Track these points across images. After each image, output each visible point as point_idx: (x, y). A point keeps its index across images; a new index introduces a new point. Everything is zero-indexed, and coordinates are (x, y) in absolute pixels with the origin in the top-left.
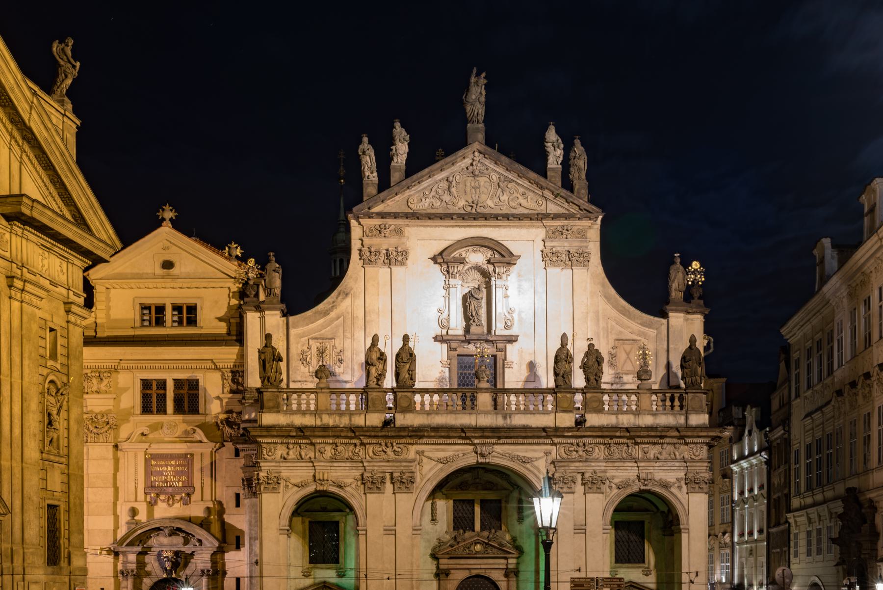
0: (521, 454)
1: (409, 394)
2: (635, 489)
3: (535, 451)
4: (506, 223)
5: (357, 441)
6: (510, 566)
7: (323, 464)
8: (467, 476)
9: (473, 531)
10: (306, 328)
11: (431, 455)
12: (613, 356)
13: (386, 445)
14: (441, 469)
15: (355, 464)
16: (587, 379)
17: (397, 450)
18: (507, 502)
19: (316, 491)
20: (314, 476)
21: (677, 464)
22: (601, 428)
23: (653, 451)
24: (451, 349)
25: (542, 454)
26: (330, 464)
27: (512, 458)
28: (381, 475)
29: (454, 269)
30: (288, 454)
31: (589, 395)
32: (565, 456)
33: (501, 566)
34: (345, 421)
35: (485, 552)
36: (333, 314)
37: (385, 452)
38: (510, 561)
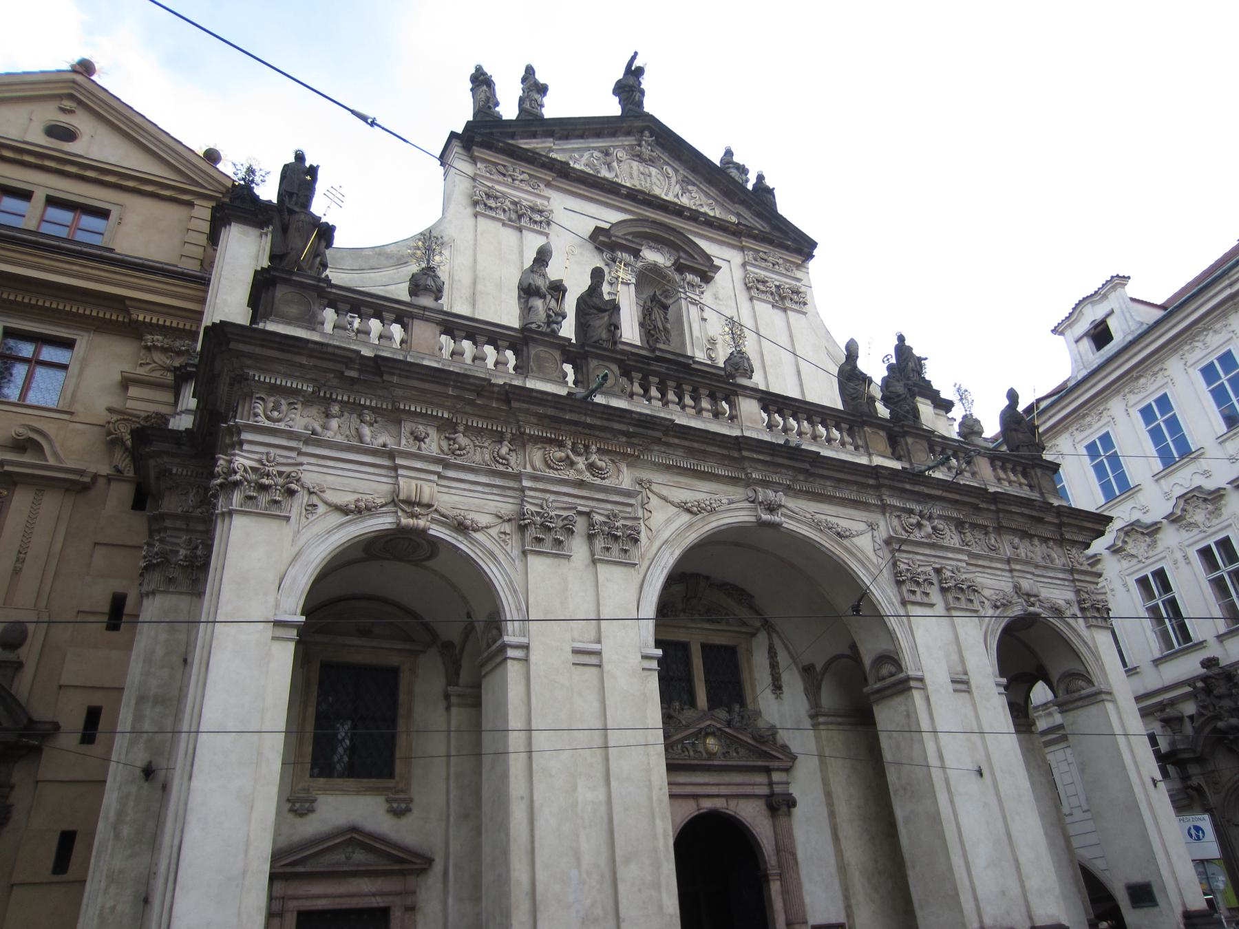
0: (829, 518)
5: (509, 431)
6: (777, 789)
7: (419, 465)
9: (693, 703)
11: (664, 491)
14: (691, 525)
15: (498, 482)
17: (600, 463)
18: (750, 652)
20: (396, 492)
21: (1061, 576)
23: (1024, 549)
25: (863, 527)
26: (439, 469)
27: (817, 526)
28: (565, 514)
30: (325, 427)
35: (726, 754)
37: (572, 464)
38: (776, 777)
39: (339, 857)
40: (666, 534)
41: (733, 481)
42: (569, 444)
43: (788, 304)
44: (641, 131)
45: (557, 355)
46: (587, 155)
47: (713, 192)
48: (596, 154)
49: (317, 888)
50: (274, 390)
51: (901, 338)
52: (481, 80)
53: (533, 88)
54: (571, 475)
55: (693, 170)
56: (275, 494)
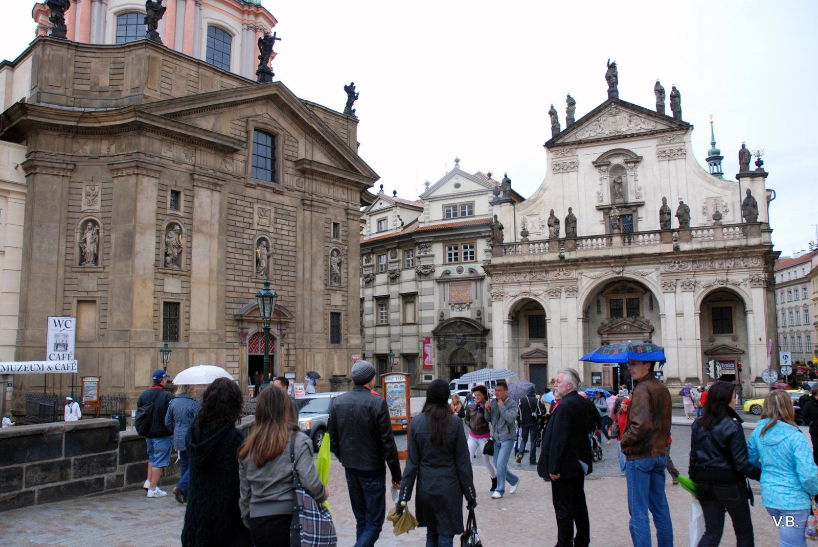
0: (640, 271)
1: (573, 241)
2: (715, 287)
3: (649, 268)
4: (633, 139)
8: (616, 286)
9: (622, 317)
10: (524, 211)
11: (587, 274)
12: (704, 208)
13: (559, 270)
14: (593, 283)
16: (681, 223)
18: (642, 300)
19: (523, 300)
22: (688, 252)
24: (605, 214)
25: (654, 270)
29: (604, 168)
31: (681, 233)
32: (668, 270)
33: (640, 338)
34: (537, 259)
35: (630, 330)
36: (538, 202)
38: (645, 334)
39: (536, 354)
40: (587, 286)
41: (607, 267)
42: (558, 270)
43: (676, 157)
44: (611, 103)
45: (557, 243)
46: (590, 126)
47: (643, 116)
48: (595, 123)
49: (532, 360)
50: (496, 274)
51: (743, 146)
52: (553, 113)
53: (571, 102)
54: (560, 277)
55: (634, 110)
56: (499, 296)
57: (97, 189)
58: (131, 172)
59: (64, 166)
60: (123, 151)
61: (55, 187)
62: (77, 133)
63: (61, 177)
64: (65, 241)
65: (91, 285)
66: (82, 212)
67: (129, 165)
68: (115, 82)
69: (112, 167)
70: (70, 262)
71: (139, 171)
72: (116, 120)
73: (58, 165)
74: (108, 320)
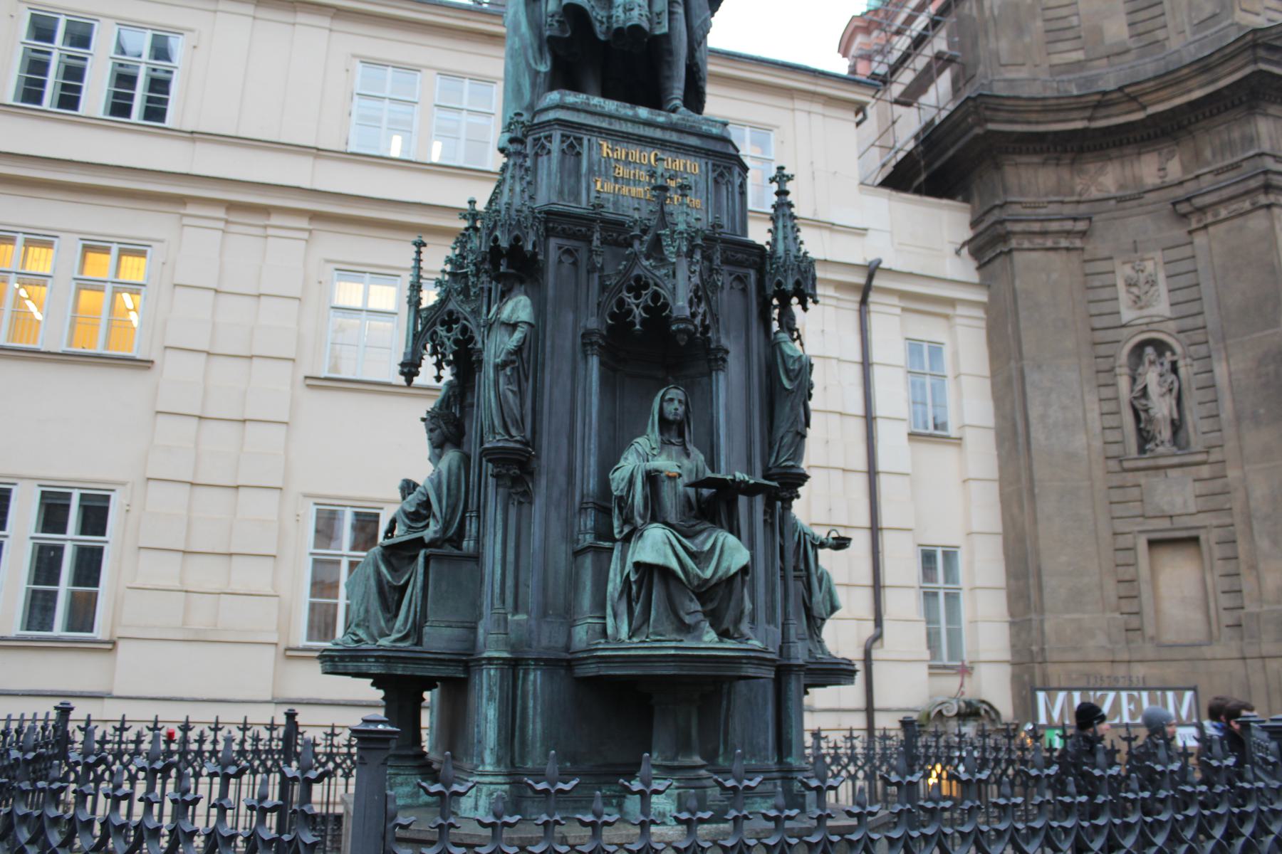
57: (1149, 266)
58: (1247, 205)
59: (1068, 225)
60: (1208, 164)
61: (1055, 276)
62: (1082, 150)
63: (1064, 252)
64: (1096, 399)
65: (1179, 500)
66: (1124, 326)
67: (1241, 188)
68: (1141, 28)
69: (1184, 208)
70: (1115, 447)
71: (1272, 198)
72: (1190, 91)
73: (1054, 226)
74: (1248, 583)
